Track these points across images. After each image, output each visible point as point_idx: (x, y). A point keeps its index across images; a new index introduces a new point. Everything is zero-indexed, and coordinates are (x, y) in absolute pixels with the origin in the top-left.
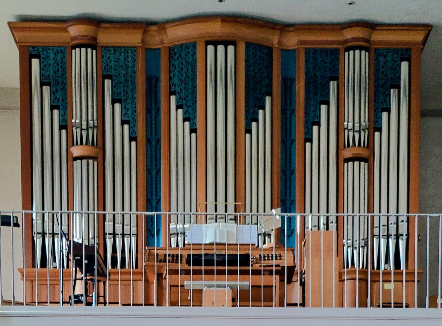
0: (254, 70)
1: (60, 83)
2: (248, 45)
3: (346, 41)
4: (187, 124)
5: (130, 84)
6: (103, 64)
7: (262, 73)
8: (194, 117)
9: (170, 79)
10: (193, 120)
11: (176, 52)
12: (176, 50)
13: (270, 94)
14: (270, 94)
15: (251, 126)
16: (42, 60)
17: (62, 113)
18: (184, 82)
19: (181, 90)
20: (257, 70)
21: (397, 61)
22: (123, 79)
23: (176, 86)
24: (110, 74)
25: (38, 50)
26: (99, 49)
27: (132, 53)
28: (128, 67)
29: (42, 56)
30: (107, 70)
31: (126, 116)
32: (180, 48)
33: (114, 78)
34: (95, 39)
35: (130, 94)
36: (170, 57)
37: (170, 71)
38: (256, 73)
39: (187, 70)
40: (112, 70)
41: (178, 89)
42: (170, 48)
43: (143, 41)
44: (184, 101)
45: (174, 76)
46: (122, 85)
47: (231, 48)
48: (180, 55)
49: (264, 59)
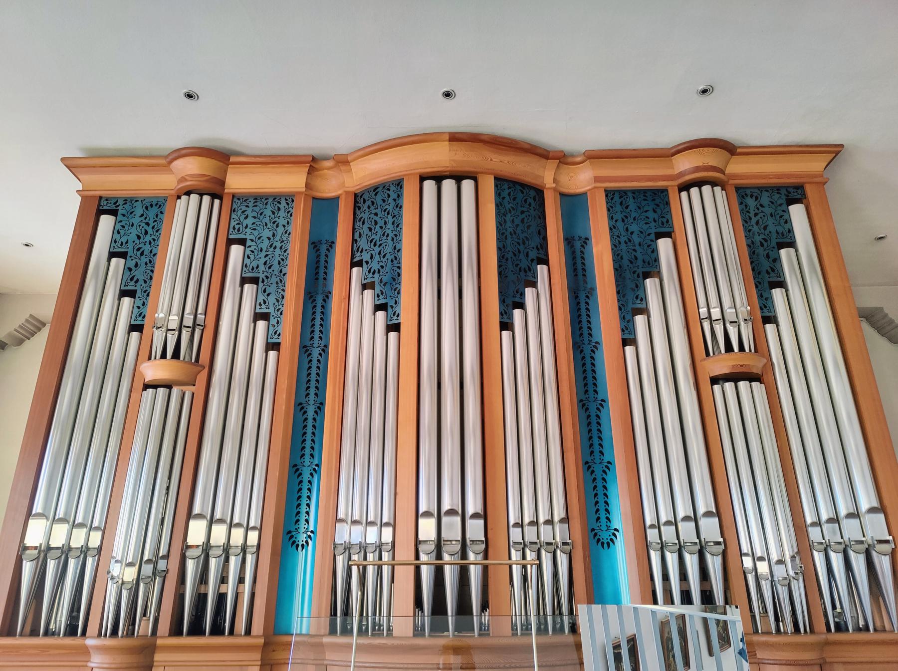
0: (513, 221)
1: (145, 253)
2: (500, 181)
3: (681, 174)
4: (381, 315)
5: (278, 251)
6: (232, 221)
7: (528, 227)
8: (396, 303)
9: (354, 241)
10: (392, 307)
11: (367, 199)
12: (366, 196)
13: (546, 262)
14: (546, 262)
15: (511, 317)
16: (120, 217)
17: (139, 303)
18: (378, 243)
19: (372, 257)
20: (517, 221)
21: (781, 205)
22: (265, 245)
23: (364, 253)
24: (242, 236)
25: (115, 203)
26: (227, 201)
27: (288, 204)
29: (120, 212)
30: (239, 230)
31: (263, 306)
32: (374, 191)
33: (249, 243)
34: (222, 183)
35: (276, 267)
36: (356, 207)
37: (354, 229)
38: (517, 226)
39: (385, 223)
40: (248, 230)
41: (366, 257)
42: (356, 195)
43: (308, 185)
44: (377, 275)
45: (360, 236)
46: (264, 253)
47: (468, 186)
48: (373, 203)
49: (530, 205)
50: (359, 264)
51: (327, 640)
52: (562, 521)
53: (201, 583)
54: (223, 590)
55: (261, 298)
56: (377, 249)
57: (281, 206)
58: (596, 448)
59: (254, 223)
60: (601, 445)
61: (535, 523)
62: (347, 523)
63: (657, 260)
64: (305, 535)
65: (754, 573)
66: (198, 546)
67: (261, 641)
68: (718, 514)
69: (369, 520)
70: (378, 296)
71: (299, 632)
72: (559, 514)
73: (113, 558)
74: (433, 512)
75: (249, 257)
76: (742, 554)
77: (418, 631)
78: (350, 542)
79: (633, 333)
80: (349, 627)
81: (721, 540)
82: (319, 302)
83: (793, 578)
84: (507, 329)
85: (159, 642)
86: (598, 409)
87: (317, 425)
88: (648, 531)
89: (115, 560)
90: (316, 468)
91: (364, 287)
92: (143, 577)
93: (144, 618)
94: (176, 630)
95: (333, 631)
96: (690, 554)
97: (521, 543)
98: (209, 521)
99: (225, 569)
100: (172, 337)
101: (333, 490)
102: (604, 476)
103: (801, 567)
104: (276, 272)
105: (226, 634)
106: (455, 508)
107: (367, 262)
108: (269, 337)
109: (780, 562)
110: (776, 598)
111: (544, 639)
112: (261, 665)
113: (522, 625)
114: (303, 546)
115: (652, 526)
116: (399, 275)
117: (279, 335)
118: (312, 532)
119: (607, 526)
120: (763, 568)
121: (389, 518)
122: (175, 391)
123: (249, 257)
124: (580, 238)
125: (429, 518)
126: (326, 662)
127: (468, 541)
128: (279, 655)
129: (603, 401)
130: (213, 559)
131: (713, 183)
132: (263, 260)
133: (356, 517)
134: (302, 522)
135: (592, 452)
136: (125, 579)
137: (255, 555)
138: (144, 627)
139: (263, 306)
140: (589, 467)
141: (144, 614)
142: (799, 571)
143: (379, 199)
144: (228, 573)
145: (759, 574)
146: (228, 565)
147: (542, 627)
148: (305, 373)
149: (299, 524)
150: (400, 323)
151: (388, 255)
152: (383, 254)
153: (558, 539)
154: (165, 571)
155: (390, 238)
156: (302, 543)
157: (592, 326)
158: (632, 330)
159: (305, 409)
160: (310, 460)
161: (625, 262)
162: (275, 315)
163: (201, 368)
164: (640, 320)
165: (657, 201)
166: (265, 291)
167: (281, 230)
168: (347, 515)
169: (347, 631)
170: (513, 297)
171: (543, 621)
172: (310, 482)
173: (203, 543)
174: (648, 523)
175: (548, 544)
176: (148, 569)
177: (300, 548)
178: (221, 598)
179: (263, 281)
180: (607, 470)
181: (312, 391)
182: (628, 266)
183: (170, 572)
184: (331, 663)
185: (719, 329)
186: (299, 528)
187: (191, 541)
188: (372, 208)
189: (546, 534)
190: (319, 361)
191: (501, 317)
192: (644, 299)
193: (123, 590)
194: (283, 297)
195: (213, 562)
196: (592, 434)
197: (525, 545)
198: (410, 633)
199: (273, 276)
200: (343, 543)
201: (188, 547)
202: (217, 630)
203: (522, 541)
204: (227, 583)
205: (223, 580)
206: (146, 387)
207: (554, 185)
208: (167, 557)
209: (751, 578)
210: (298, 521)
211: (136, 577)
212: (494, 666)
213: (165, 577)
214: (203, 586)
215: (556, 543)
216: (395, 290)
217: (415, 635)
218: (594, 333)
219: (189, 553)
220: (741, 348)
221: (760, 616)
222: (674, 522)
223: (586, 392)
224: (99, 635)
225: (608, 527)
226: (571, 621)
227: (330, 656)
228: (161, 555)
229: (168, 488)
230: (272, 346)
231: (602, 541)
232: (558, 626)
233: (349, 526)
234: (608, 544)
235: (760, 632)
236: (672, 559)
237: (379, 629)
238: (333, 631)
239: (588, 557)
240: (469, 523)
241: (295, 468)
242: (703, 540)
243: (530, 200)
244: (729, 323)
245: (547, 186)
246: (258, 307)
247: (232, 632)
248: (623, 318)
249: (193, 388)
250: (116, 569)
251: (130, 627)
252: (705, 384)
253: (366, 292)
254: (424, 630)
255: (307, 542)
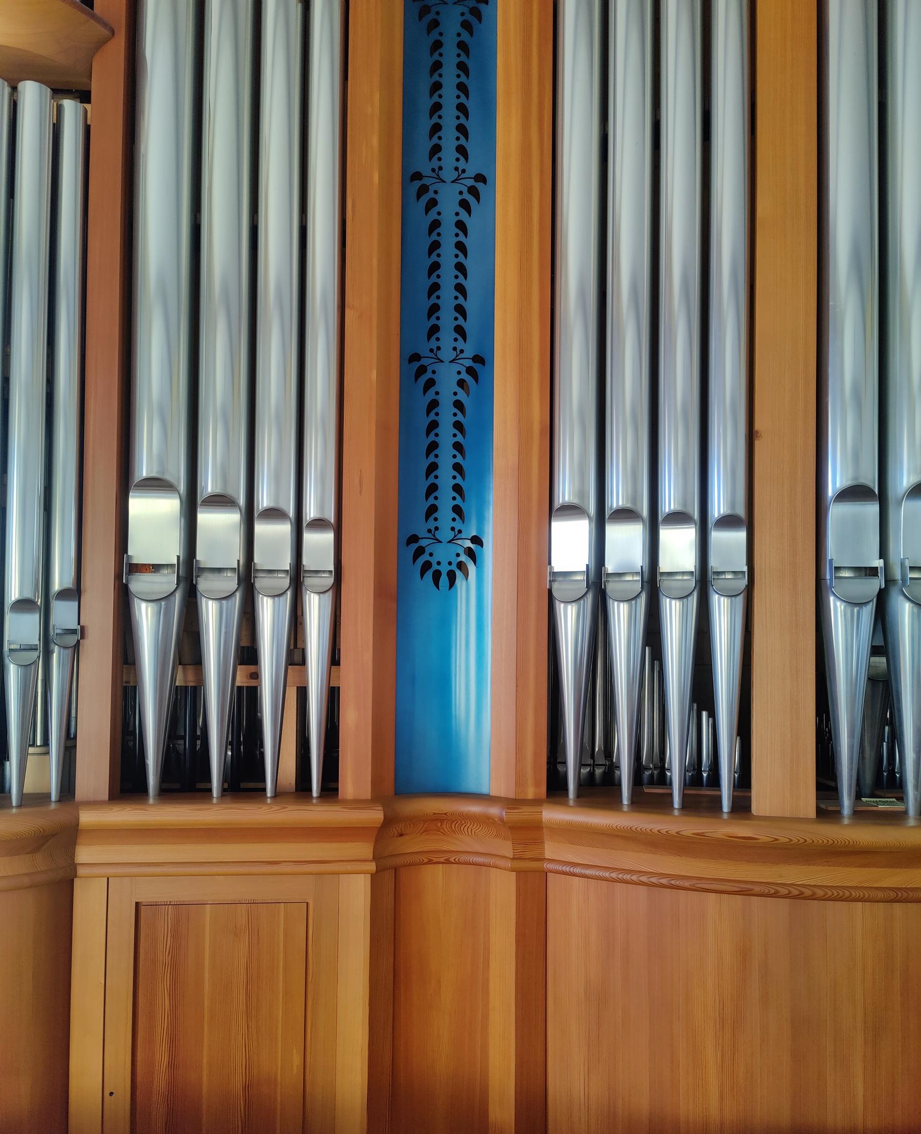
85: (87, 818)
92: (12, 647)
130: (210, 602)
137: (328, 597)
154: (74, 632)
160: (454, 344)
173: (178, 557)
195: (210, 611)
201: (136, 568)
208: (74, 593)
213: (77, 647)
219: (139, 584)
241: (416, 365)
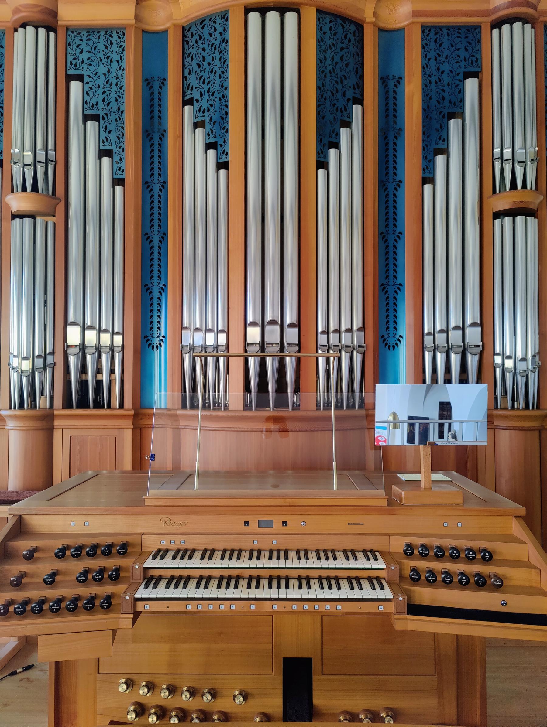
0: (333, 59)
3: (496, 10)
4: (211, 153)
6: (69, 55)
7: (347, 65)
8: (225, 142)
9: (184, 78)
10: (221, 145)
11: (194, 32)
12: (193, 30)
13: (360, 101)
14: (360, 101)
15: (326, 156)
18: (207, 81)
19: (201, 95)
20: (337, 59)
22: (102, 81)
23: (194, 90)
27: (119, 38)
28: (111, 61)
30: (76, 66)
31: (106, 143)
32: (201, 24)
33: (86, 79)
34: (54, 14)
35: (114, 104)
36: (185, 42)
37: (183, 65)
38: (336, 63)
40: (85, 66)
41: (196, 95)
43: (137, 17)
44: (206, 114)
45: (190, 73)
46: (101, 90)
48: (200, 37)
49: (349, 41)
50: (190, 102)
51: (180, 412)
52: (359, 330)
53: (82, 373)
54: (99, 377)
55: (103, 135)
56: (206, 87)
57: (113, 40)
58: (391, 273)
59: (89, 58)
60: (395, 270)
61: (338, 331)
62: (191, 330)
63: (462, 101)
64: (158, 339)
65: (501, 368)
66: (76, 346)
67: (132, 412)
68: (482, 325)
69: (208, 328)
70: (209, 135)
71: (159, 407)
72: (357, 324)
73: (11, 353)
74: (258, 322)
75: (88, 94)
76: (494, 354)
77: (247, 407)
78: (193, 344)
79: (432, 172)
80: (196, 404)
81: (481, 344)
82: (156, 140)
83: (531, 371)
84: (322, 168)
85: (56, 412)
86: (396, 240)
87: (162, 252)
88: (426, 338)
89: (12, 355)
90: (164, 287)
91: (196, 125)
92: (37, 368)
93: (42, 397)
94: (67, 404)
95: (184, 406)
96: (455, 354)
97: (326, 346)
98: (82, 327)
99: (99, 364)
100: (29, 171)
101: (178, 305)
102: (396, 295)
103: (538, 363)
104: (114, 109)
105: (105, 408)
106: (275, 319)
107: (197, 101)
108: (114, 174)
109: (523, 359)
110: (515, 385)
111: (340, 413)
112: (133, 428)
113: (324, 404)
114: (157, 347)
115: (429, 334)
116: (227, 114)
117: (123, 171)
118: (163, 337)
119: (394, 333)
120: (509, 364)
121: (224, 327)
122: (39, 220)
123: (88, 94)
124: (394, 76)
125: (255, 327)
126: (180, 427)
127: (285, 344)
128: (145, 422)
129: (400, 285)
130: (89, 355)
131: (524, 20)
132: (101, 97)
133: (198, 326)
134: (155, 329)
135: (387, 276)
136: (23, 369)
137: (121, 353)
138: (43, 403)
139: (106, 143)
140: (384, 288)
141: (42, 393)
142: (536, 366)
143: (206, 32)
144: (101, 365)
145: (505, 368)
146: (101, 361)
147: (339, 405)
148: (149, 207)
149: (153, 331)
150: (229, 161)
151: (216, 94)
152: (211, 93)
153: (355, 342)
154: (53, 363)
155: (217, 75)
156: (157, 345)
157: (397, 217)
158: (432, 170)
159: (151, 239)
160: (158, 281)
161: (434, 102)
162: (117, 152)
163: (58, 201)
164: (440, 160)
165: (469, 39)
166: (106, 128)
167: (115, 65)
168: (190, 324)
169: (194, 406)
170: (329, 137)
171: (340, 401)
172: (159, 298)
173: (80, 343)
174: (426, 331)
175: (347, 346)
176: (39, 362)
177: (155, 348)
178: (99, 384)
179: (103, 119)
180: (398, 290)
181: (156, 222)
182: (435, 106)
183: (57, 364)
184: (184, 427)
185: (508, 168)
186: (153, 334)
187: (70, 341)
188: (200, 42)
189: (346, 339)
190: (159, 196)
191: (318, 156)
192: (446, 140)
193: (23, 377)
194: (123, 135)
195: (89, 358)
196: (389, 307)
197: (329, 347)
198: (241, 407)
199: (113, 114)
200: (188, 345)
201: (68, 346)
202: (98, 404)
203: (327, 345)
204: (102, 373)
205: (99, 370)
206: (14, 217)
207: (374, 20)
208: (53, 353)
209: (498, 371)
210: (152, 328)
211: (31, 368)
212: (303, 430)
213: (54, 367)
214: (84, 375)
215: (354, 346)
216: (224, 129)
217: (245, 410)
218: (398, 172)
219: (70, 351)
220: (524, 186)
221: (501, 397)
222: (446, 330)
223: (387, 225)
224: (10, 408)
225: (395, 335)
226: (361, 401)
227: (183, 423)
228: (48, 352)
229: (46, 302)
230: (117, 182)
231: (389, 344)
232: (351, 404)
233: (192, 332)
234: (394, 347)
235: (499, 408)
236: (440, 358)
237: (218, 406)
238: (184, 406)
239: (377, 356)
240: (287, 330)
241: (147, 287)
242: (466, 343)
243: (350, 36)
244: (517, 162)
245: (367, 20)
246: (101, 144)
247: (109, 406)
248: (425, 158)
249: (54, 219)
250: (15, 362)
251: (33, 403)
252: (488, 217)
253: (197, 130)
254: (252, 406)
255: (160, 344)
